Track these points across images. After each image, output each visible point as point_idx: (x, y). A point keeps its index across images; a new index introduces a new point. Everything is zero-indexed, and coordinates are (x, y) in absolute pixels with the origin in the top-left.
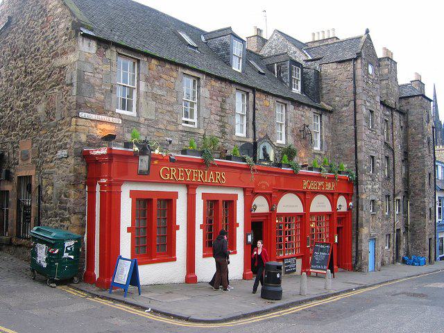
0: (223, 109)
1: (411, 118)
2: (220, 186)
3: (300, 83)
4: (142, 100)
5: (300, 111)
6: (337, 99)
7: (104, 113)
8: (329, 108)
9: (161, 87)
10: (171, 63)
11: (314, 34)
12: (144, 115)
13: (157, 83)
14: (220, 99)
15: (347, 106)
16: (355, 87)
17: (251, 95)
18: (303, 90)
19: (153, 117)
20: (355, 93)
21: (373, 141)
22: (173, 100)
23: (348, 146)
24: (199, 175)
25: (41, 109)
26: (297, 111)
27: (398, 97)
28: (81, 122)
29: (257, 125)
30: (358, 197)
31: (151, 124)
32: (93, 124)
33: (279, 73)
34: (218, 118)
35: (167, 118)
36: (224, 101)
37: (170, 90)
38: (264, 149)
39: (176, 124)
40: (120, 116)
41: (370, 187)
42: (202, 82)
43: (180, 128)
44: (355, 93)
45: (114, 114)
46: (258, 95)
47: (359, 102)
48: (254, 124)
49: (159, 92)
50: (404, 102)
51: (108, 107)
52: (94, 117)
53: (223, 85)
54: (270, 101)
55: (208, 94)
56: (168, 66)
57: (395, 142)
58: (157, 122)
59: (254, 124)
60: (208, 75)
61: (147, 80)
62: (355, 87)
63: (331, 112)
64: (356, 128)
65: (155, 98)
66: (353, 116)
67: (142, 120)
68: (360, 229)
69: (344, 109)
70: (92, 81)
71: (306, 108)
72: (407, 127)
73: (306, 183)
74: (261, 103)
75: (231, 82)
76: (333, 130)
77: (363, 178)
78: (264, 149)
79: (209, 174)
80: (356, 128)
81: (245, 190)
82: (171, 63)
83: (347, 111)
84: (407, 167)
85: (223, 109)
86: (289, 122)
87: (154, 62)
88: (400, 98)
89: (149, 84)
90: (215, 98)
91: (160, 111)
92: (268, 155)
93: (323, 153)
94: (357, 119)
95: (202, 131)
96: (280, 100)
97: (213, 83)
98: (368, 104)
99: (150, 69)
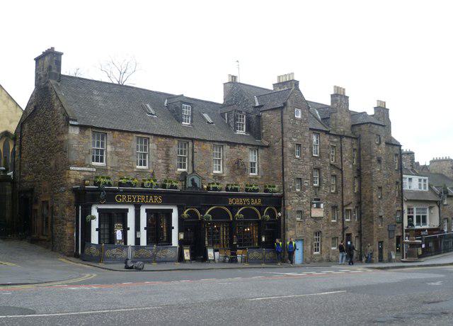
0: (167, 155)
1: (362, 141)
2: (157, 204)
3: (245, 126)
4: (108, 156)
5: (236, 149)
6: (272, 136)
7: (85, 166)
8: (267, 143)
9: (121, 147)
11: (279, 77)
12: (109, 164)
13: (119, 145)
15: (278, 142)
16: (282, 129)
17: (190, 144)
18: (248, 130)
20: (282, 133)
21: (299, 167)
22: (130, 154)
23: (278, 172)
25: (52, 163)
27: (349, 125)
28: (71, 172)
29: (195, 162)
30: (284, 209)
31: (114, 169)
32: (78, 173)
33: (228, 120)
34: (164, 161)
35: (126, 165)
36: (168, 150)
37: (127, 148)
38: (193, 180)
39: (132, 168)
40: (94, 167)
41: (297, 201)
42: (151, 140)
43: (135, 170)
44: (282, 133)
45: (91, 166)
46: (196, 143)
47: (285, 139)
48: (193, 162)
49: (120, 150)
50: (357, 129)
51: (87, 162)
52: (79, 169)
53: (167, 140)
54: (208, 146)
55: (155, 147)
56: (126, 134)
57: (344, 164)
58: (119, 168)
59: (193, 162)
61: (112, 144)
62: (282, 129)
63: (267, 147)
64: (283, 158)
65: (117, 154)
66: (281, 150)
67: (109, 168)
68: (287, 232)
69: (277, 144)
70: (77, 149)
72: (360, 149)
73: (231, 201)
76: (268, 159)
77: (288, 194)
78: (193, 180)
79: (149, 198)
80: (283, 158)
83: (278, 146)
84: (360, 182)
85: (167, 155)
86: (225, 158)
87: (116, 133)
88: (353, 126)
93: (260, 177)
94: (284, 151)
95: (151, 171)
96: (217, 144)
97: (160, 139)
98: (294, 140)
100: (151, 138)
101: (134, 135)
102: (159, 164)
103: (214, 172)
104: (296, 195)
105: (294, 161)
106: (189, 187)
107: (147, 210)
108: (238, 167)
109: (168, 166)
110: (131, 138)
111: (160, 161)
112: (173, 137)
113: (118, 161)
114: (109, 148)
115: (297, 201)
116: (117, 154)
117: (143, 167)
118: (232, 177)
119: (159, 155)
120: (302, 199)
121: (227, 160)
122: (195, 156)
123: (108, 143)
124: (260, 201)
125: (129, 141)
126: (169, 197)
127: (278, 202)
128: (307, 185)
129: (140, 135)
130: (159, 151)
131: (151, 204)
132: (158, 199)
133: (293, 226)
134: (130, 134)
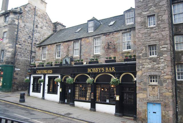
0: (68, 50)
10: (53, 44)
14: (67, 47)
21: (152, 35)
24: (45, 72)
26: (108, 37)
29: (83, 51)
35: (52, 58)
36: (69, 47)
42: (61, 45)
43: (55, 59)
53: (69, 42)
60: (63, 42)
61: (48, 50)
65: (49, 54)
67: (46, 60)
71: (115, 33)
73: (89, 70)
74: (85, 42)
75: (71, 41)
78: (66, 60)
79: (47, 71)
81: (61, 75)
82: (53, 44)
85: (68, 50)
87: (49, 45)
95: (61, 59)
97: (65, 43)
100: (62, 44)
101: (55, 44)
103: (94, 54)
104: (148, 61)
105: (146, 31)
108: (109, 47)
110: (54, 46)
111: (65, 54)
112: (71, 41)
114: (46, 52)
115: (150, 66)
118: (107, 55)
120: (158, 64)
121: (103, 45)
122: (82, 47)
124: (113, 68)
126: (55, 71)
127: (133, 68)
128: (165, 49)
129: (57, 44)
131: (50, 74)
132: (51, 71)
133: (145, 90)
134: (54, 45)
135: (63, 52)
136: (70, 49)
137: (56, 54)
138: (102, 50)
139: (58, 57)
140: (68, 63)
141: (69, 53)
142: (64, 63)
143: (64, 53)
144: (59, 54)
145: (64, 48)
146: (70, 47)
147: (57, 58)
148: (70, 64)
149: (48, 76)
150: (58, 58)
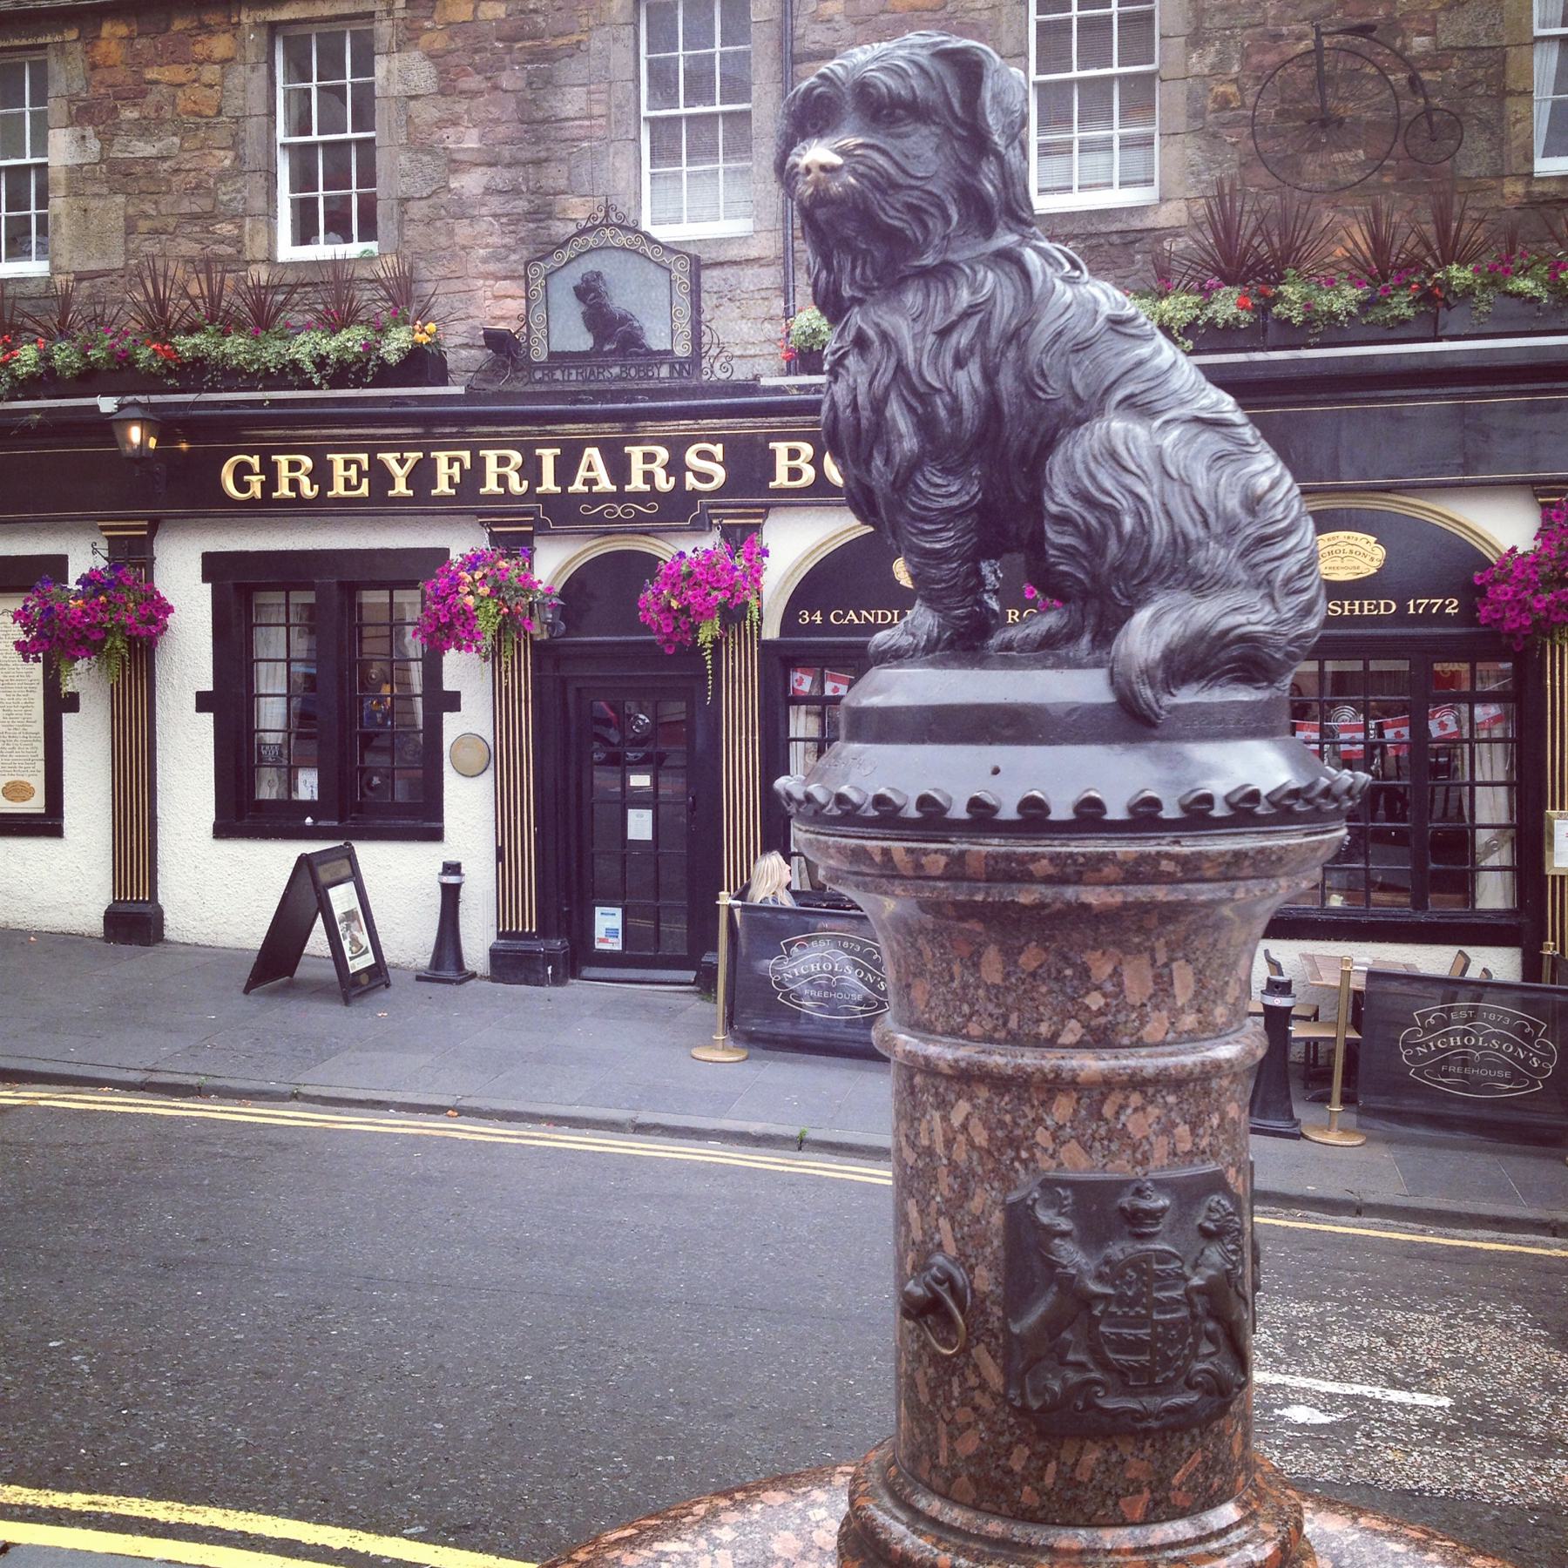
9: (144, 129)
13: (130, 114)
19: (118, 263)
34: (502, 177)
36: (545, 83)
37: (195, 124)
43: (261, 274)
55: (422, 75)
61: (82, 114)
65: (121, 176)
89: (89, 131)
90: (473, 82)
91: (144, 225)
92: (625, 319)
99: (94, 67)
102: (462, 210)
106: (560, 359)
107: (214, 567)
109: (542, 213)
110: (220, 45)
113: (130, 230)
116: (121, 176)
117: (354, 249)
119: (471, 140)
121: (1200, 62)
123: (56, 108)
125: (210, 73)
130: (461, 107)
135: (428, 150)
136: (571, 103)
137: (272, 177)
138: (1190, 150)
139: (304, 235)
140: (657, 338)
141: (554, 176)
142: (559, 345)
143: (455, 165)
144: (367, 178)
145: (446, 90)
146: (571, 70)
147: (287, 251)
148: (682, 350)
149: (208, 559)
150: (322, 250)
